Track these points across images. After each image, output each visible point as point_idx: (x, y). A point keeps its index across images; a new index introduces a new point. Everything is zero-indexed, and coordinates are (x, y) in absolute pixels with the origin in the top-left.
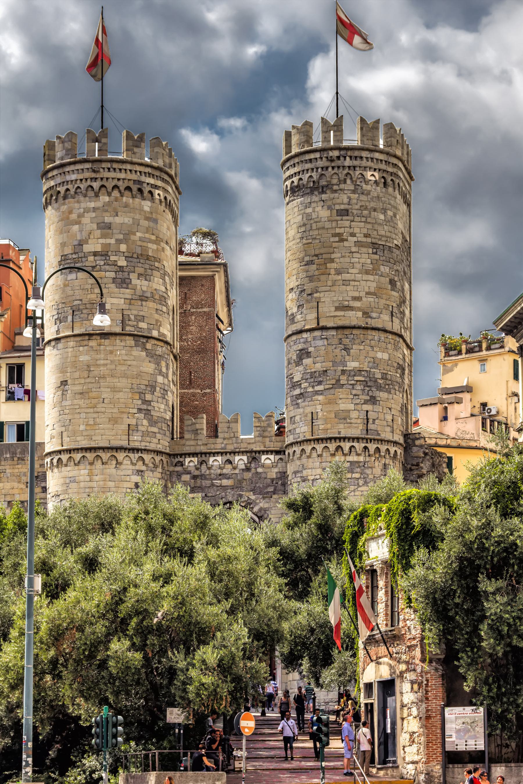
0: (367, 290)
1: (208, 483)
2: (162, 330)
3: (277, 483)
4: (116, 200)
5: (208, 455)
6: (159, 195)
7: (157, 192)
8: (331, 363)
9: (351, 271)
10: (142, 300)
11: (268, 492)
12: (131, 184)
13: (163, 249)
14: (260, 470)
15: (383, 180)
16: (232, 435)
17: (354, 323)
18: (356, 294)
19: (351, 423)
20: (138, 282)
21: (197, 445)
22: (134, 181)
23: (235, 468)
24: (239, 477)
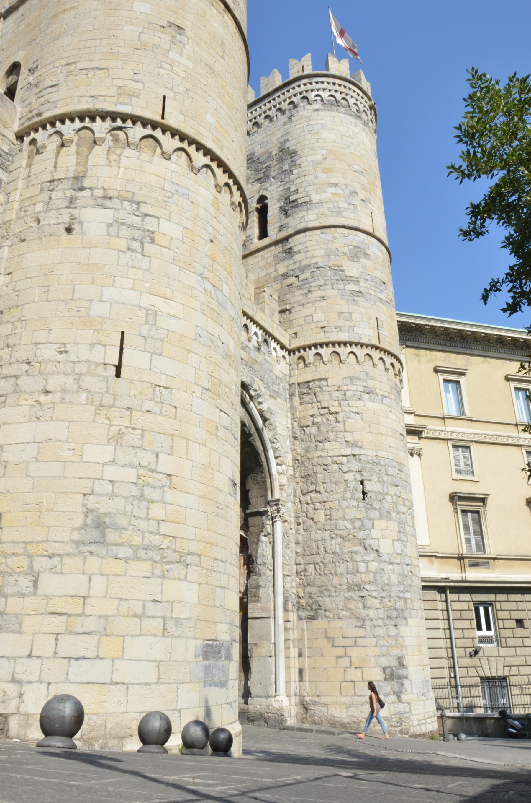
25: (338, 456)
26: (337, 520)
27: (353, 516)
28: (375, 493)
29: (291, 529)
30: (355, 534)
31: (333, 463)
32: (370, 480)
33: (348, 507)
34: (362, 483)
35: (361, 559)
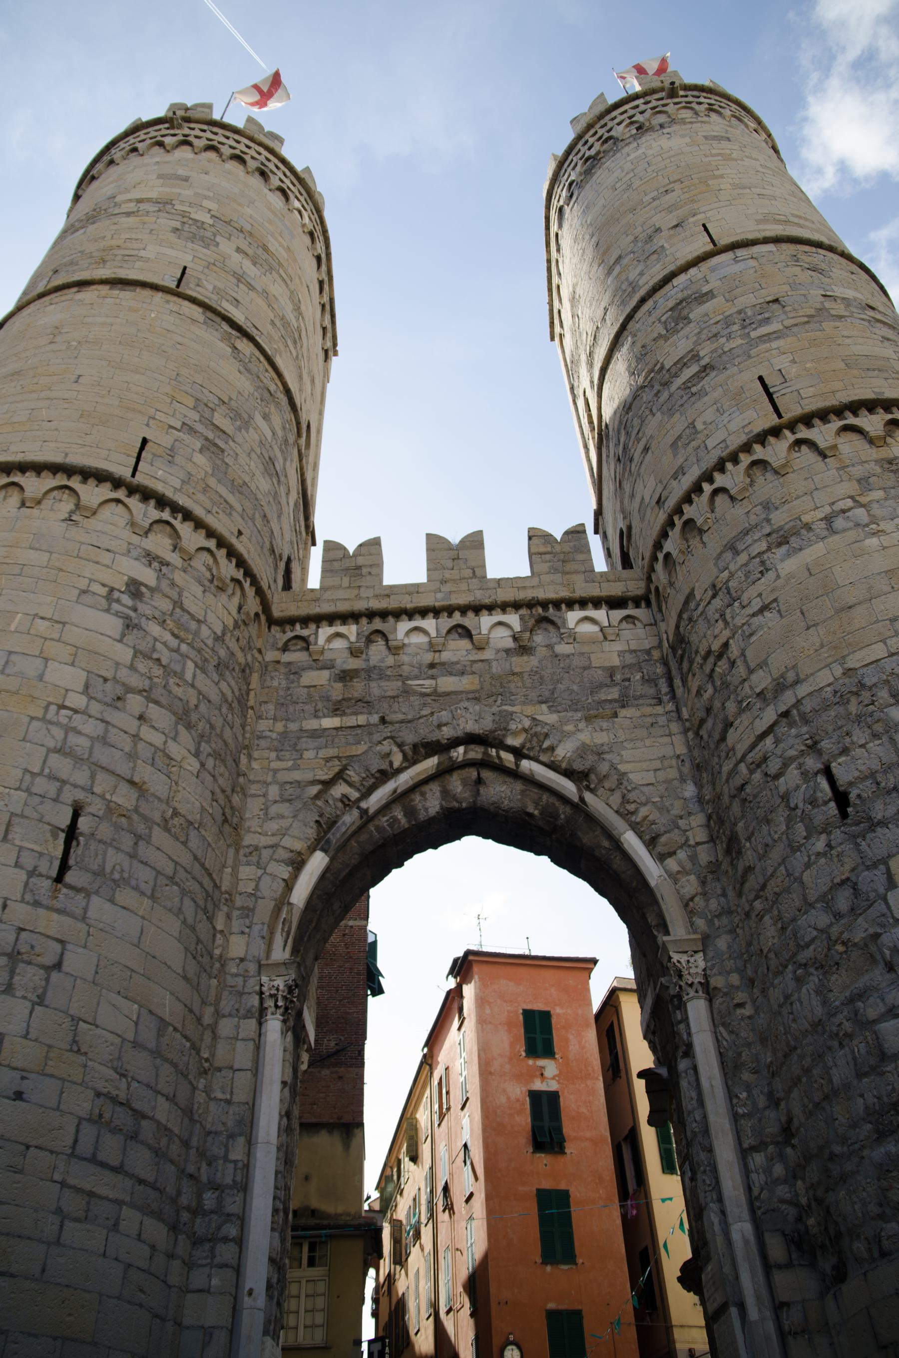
1: (392, 687)
3: (629, 680)
4: (209, 161)
5: (391, 619)
6: (300, 212)
7: (297, 204)
8: (786, 288)
10: (239, 281)
11: (601, 703)
12: (247, 158)
14: (563, 649)
16: (468, 573)
20: (236, 258)
21: (358, 597)
22: (253, 158)
23: (481, 649)
24: (496, 668)
25: (753, 747)
26: (794, 920)
27: (824, 884)
28: (873, 774)
29: (741, 1005)
30: (845, 936)
31: (751, 772)
32: (845, 751)
33: (808, 866)
34: (827, 772)
35: (882, 1009)
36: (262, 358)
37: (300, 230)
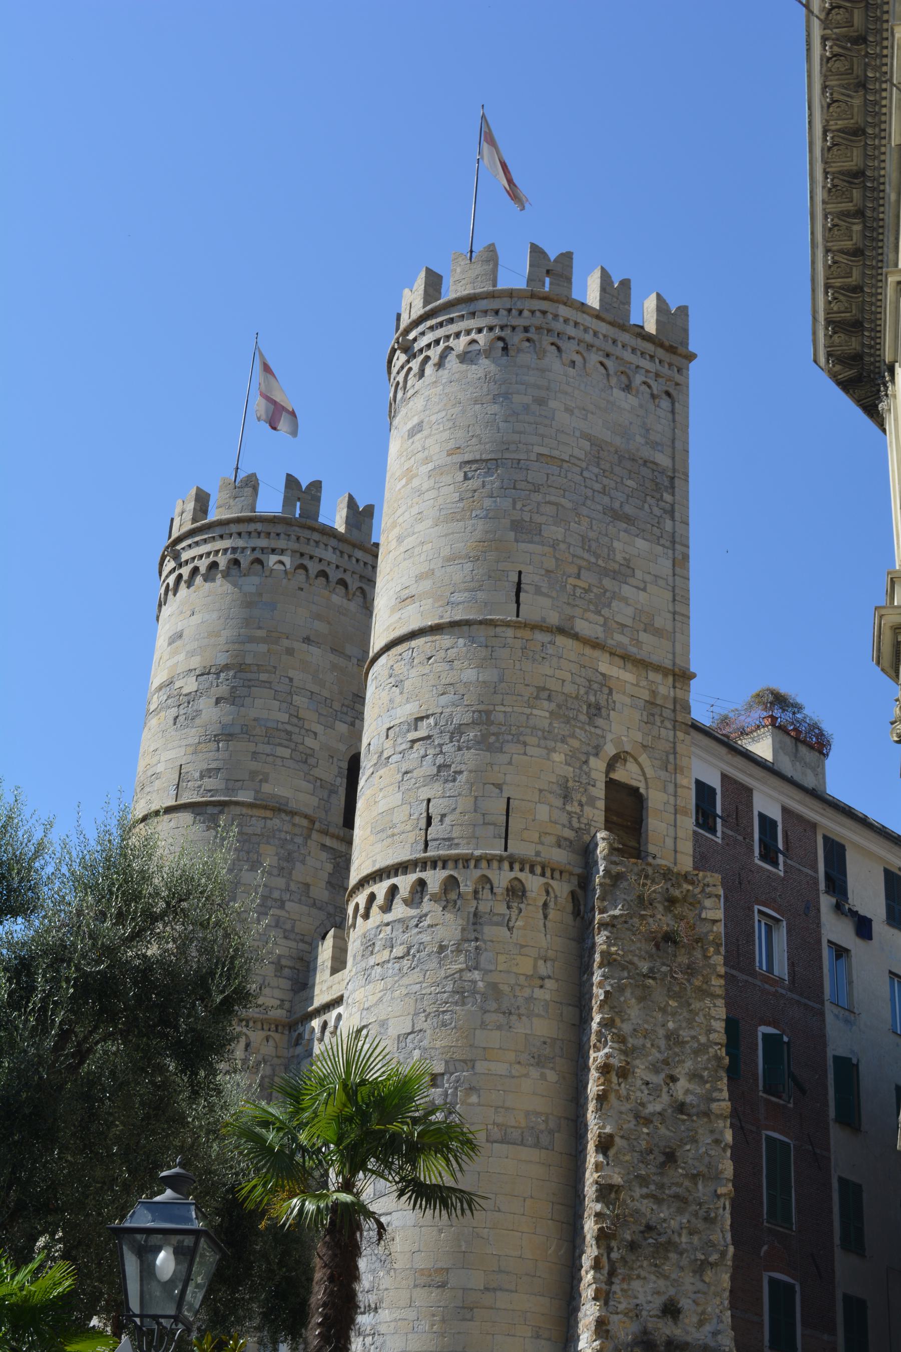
0: (446, 552)
2: (267, 788)
7: (273, 558)
9: (419, 527)
13: (290, 652)
15: (501, 344)
17: (415, 625)
18: (424, 568)
19: (393, 835)
36: (244, 811)
37: (285, 581)
